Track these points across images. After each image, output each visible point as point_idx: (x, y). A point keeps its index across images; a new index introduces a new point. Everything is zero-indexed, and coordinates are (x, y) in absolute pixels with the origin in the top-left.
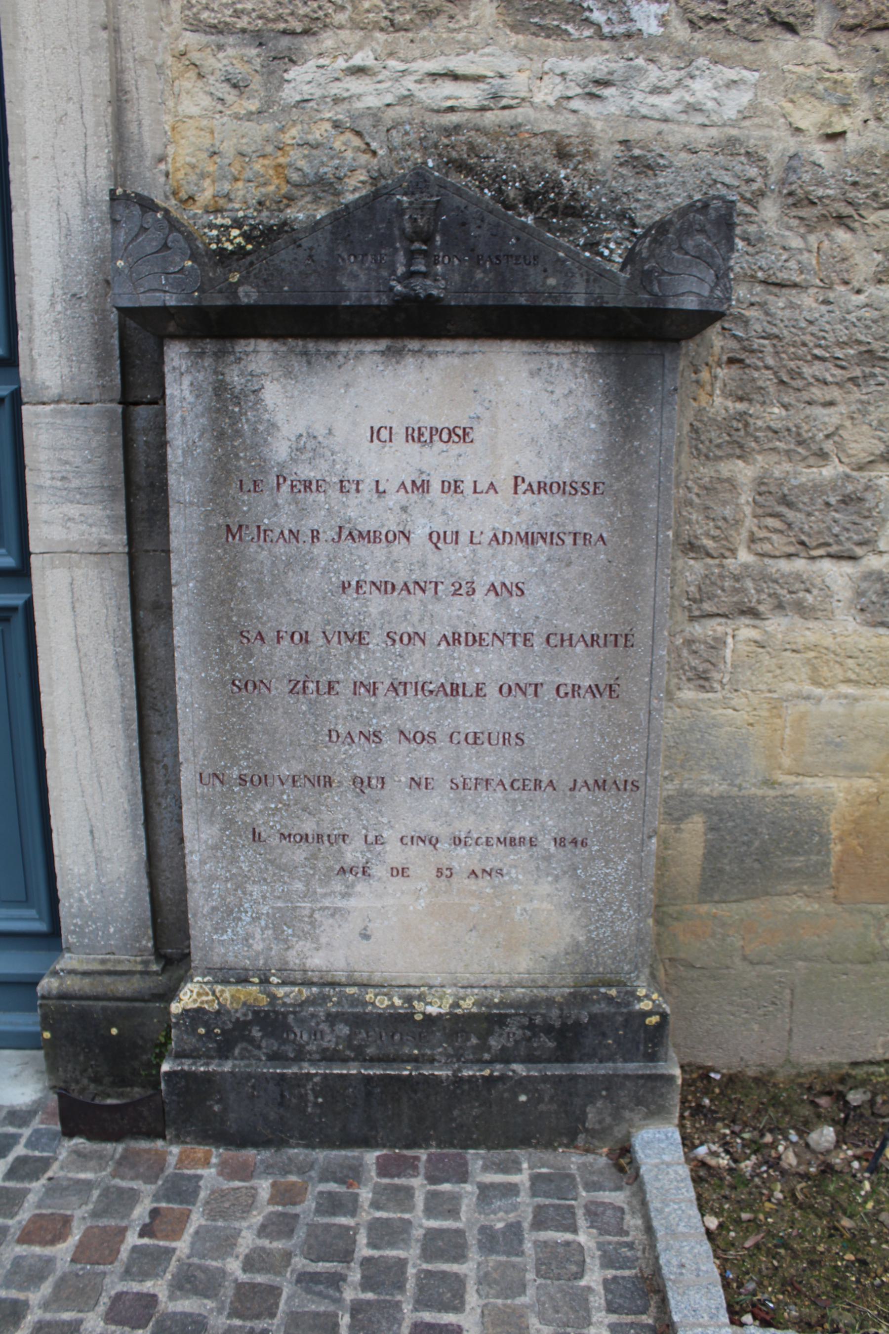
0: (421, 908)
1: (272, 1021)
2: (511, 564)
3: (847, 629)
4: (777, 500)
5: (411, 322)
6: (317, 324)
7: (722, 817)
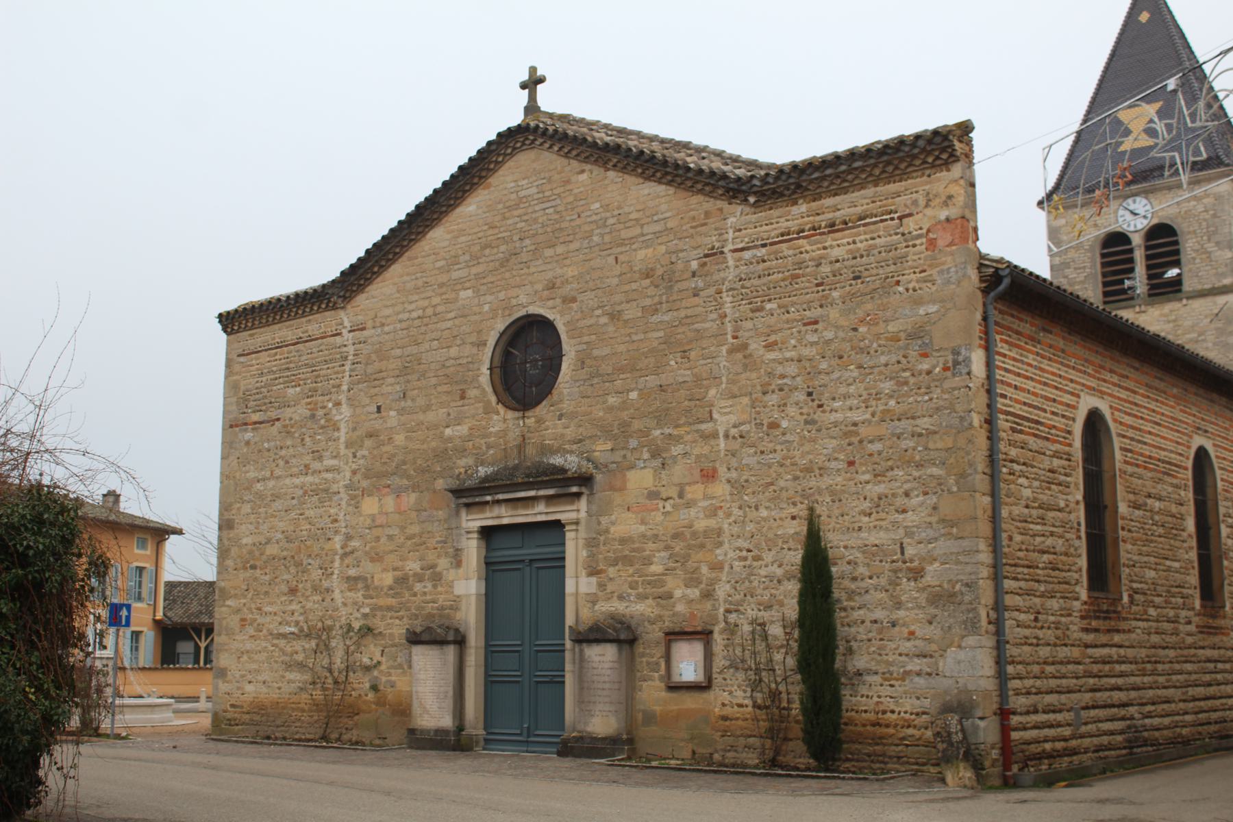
0: (602, 723)
1: (582, 738)
2: (609, 672)
3: (657, 683)
4: (648, 663)
5: (598, 641)
6: (590, 641)
7: (644, 712)
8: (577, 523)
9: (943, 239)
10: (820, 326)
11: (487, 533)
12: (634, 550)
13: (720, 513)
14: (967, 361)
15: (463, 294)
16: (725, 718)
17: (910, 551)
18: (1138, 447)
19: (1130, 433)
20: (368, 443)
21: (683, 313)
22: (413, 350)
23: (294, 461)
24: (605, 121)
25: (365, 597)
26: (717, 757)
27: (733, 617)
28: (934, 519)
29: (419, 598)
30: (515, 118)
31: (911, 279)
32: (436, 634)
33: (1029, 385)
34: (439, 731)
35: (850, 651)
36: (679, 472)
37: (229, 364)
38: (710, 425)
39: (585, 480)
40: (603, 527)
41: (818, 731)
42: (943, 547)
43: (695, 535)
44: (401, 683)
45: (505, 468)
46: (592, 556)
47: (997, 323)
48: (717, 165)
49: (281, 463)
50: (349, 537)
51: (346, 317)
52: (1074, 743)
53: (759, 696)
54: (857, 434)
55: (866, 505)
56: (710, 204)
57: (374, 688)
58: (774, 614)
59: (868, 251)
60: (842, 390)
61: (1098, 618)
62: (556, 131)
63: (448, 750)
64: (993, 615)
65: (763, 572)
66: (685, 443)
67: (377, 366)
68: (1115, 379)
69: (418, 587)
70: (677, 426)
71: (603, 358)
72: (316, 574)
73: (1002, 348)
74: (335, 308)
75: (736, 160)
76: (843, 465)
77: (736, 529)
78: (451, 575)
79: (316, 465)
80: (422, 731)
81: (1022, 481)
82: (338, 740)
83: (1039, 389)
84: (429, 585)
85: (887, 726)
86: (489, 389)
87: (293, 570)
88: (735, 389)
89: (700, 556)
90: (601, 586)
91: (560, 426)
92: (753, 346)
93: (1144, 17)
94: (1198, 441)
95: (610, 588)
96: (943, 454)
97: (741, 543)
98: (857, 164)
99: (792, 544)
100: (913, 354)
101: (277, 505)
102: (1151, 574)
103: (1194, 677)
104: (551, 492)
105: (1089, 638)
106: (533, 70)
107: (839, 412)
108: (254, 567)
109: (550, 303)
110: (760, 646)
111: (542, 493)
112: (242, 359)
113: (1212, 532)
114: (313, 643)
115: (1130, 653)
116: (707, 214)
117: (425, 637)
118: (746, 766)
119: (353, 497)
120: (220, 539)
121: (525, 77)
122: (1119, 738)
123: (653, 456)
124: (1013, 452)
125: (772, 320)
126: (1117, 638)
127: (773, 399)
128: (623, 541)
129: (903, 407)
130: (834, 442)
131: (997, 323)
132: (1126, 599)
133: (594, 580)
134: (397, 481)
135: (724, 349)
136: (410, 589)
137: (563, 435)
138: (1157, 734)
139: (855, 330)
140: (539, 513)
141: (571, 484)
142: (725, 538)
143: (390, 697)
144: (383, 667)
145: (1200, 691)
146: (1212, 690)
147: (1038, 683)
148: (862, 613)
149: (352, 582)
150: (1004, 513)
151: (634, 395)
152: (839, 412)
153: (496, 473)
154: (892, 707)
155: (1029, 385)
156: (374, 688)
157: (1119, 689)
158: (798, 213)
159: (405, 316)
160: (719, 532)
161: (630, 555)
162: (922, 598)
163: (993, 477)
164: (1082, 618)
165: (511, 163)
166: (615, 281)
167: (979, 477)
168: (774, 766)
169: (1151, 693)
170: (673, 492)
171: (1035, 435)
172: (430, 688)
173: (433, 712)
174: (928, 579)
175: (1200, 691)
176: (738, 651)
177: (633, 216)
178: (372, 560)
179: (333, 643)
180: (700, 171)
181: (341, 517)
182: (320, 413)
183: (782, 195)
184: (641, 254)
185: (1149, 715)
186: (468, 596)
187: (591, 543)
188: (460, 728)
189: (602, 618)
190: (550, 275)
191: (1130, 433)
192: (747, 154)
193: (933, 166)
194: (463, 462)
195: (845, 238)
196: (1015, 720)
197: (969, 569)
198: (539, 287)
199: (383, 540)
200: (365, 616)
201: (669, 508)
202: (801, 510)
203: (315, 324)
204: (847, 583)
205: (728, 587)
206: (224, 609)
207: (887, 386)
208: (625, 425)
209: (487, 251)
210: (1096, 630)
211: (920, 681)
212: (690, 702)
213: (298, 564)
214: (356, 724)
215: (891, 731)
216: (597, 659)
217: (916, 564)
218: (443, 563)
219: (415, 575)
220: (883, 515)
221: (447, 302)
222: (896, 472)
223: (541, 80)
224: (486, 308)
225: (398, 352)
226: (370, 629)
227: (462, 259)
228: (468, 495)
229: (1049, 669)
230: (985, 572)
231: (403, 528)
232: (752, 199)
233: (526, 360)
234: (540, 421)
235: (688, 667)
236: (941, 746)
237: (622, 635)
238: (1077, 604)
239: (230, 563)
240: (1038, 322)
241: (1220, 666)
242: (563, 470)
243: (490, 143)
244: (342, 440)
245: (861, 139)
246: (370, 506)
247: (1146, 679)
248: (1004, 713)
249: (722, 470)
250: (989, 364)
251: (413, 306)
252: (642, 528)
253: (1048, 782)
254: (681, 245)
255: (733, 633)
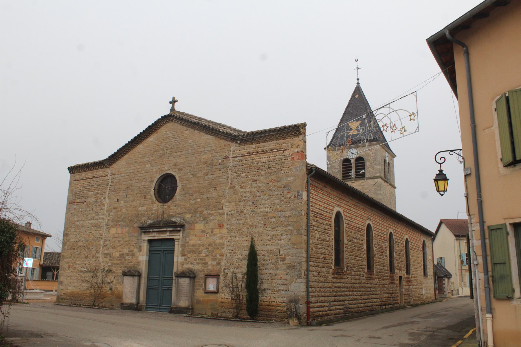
0: (183, 303)
3: (202, 291)
5: (183, 277)
6: (181, 277)
8: (179, 239)
9: (296, 158)
10: (257, 182)
11: (150, 241)
12: (196, 249)
13: (224, 238)
14: (302, 195)
15: (147, 166)
16: (222, 302)
17: (282, 252)
18: (351, 223)
19: (349, 219)
20: (114, 211)
21: (215, 176)
22: (130, 182)
23: (89, 215)
24: (195, 115)
26: (219, 315)
27: (226, 271)
28: (289, 243)
29: (127, 261)
30: (167, 112)
31: (286, 169)
32: (132, 273)
33: (320, 203)
34: (131, 304)
35: (262, 282)
36: (211, 225)
37: (70, 183)
38: (222, 210)
39: (182, 226)
40: (187, 241)
41: (251, 307)
42: (291, 251)
43: (215, 244)
44: (120, 289)
45: (157, 221)
46: (183, 250)
47: (311, 184)
48: (229, 131)
49: (85, 216)
50: (106, 241)
51: (109, 171)
52: (328, 312)
53: (233, 296)
54: (267, 215)
55: (269, 238)
56: (226, 143)
57: (111, 289)
58: (239, 270)
59: (273, 160)
60: (263, 202)
61: (337, 274)
62: (180, 117)
63: (133, 310)
64: (306, 273)
65: (236, 257)
66: (214, 216)
67: (118, 186)
68: (345, 202)
69: (127, 258)
70: (212, 211)
71: (190, 188)
72: (94, 252)
73: (312, 191)
74: (106, 168)
75: (234, 130)
76: (262, 225)
77: (228, 243)
78: (138, 254)
79: (96, 217)
80: (126, 304)
81: (316, 232)
82: (98, 306)
83: (322, 204)
84: (131, 257)
85: (272, 306)
86: (153, 196)
87: (87, 250)
88: (231, 200)
89: (217, 251)
90: (186, 260)
91: (174, 209)
92: (237, 187)
93: (357, 96)
94: (368, 222)
95: (188, 260)
96: (293, 223)
97: (230, 248)
98: (271, 134)
99: (245, 249)
100: (285, 192)
101: (83, 229)
102: (353, 261)
103: (364, 292)
104: (171, 229)
105: (334, 280)
106: (174, 98)
107: (262, 209)
108: (74, 249)
109: (174, 170)
110: (234, 280)
111: (168, 229)
112: (75, 182)
113: (371, 249)
114: (92, 274)
115: (346, 285)
116: (225, 146)
117: (128, 274)
118: (228, 318)
119: (108, 228)
120: (63, 239)
121: (171, 100)
122: (342, 311)
123: (204, 220)
124: (314, 223)
125: (243, 179)
126: (342, 280)
127: (242, 204)
128: (193, 246)
129: (280, 209)
130: (260, 218)
131: (311, 184)
132: (345, 269)
133: (183, 257)
134: (122, 223)
135: (228, 188)
136: (124, 258)
137: (176, 212)
138: (353, 310)
139: (268, 184)
140: (167, 236)
141: (177, 227)
142: (225, 246)
143: (116, 292)
144: (114, 283)
145: (366, 297)
146: (369, 297)
147: (319, 294)
148: (267, 271)
149: (106, 255)
150: (311, 242)
151: (199, 200)
152: (262, 209)
153: (154, 222)
154: (274, 300)
155: (320, 203)
156: (111, 289)
157: (342, 296)
158: (252, 147)
159: (128, 171)
160: (223, 244)
161: (195, 250)
162: (285, 267)
163: (308, 230)
164: (332, 274)
165: (165, 126)
166: (195, 164)
167: (304, 230)
168: (237, 318)
169: (352, 297)
170: (210, 231)
171: (321, 218)
172: (128, 290)
173: (130, 298)
174: (287, 261)
175: (366, 297)
176: (227, 282)
177: (202, 145)
178: (113, 248)
179: (98, 274)
180: (223, 132)
181: (103, 234)
182: (99, 200)
183: (248, 141)
184: (204, 157)
185: (351, 304)
186: (143, 261)
187: (183, 246)
188: (138, 303)
189: (185, 270)
190: (175, 161)
191: (349, 219)
192: (238, 128)
193: (294, 135)
194: (144, 218)
195: (266, 155)
196: (311, 305)
197: (299, 258)
198: (171, 165)
199: (117, 242)
200: (109, 266)
201: (208, 236)
202: (249, 238)
203: (99, 172)
204: (262, 261)
205: (225, 261)
207: (277, 201)
208: (195, 209)
209: (156, 153)
210: (336, 278)
211: (283, 292)
212: (212, 297)
213: (88, 249)
214: (104, 301)
215: (274, 308)
216: (183, 283)
217: (283, 256)
218: (135, 250)
219: (126, 254)
220: (274, 241)
221: (142, 168)
222: (278, 228)
223: (176, 101)
224: (154, 170)
225: (125, 183)
226: (110, 270)
227: (148, 155)
228: (145, 229)
229: (322, 289)
230: (304, 259)
231: (123, 239)
232: (239, 142)
233: (166, 187)
234: (169, 207)
235: (211, 286)
236: (288, 313)
237: (191, 275)
238: (331, 270)
239: (66, 247)
240: (323, 184)
241: (372, 289)
242: (175, 223)
243: (159, 119)
244: (106, 209)
245: (273, 126)
246: (113, 231)
247: (350, 293)
248: (308, 303)
249: (225, 225)
250: (308, 196)
251: (131, 169)
252: (199, 242)
253: (320, 324)
254: (216, 155)
255: (226, 276)
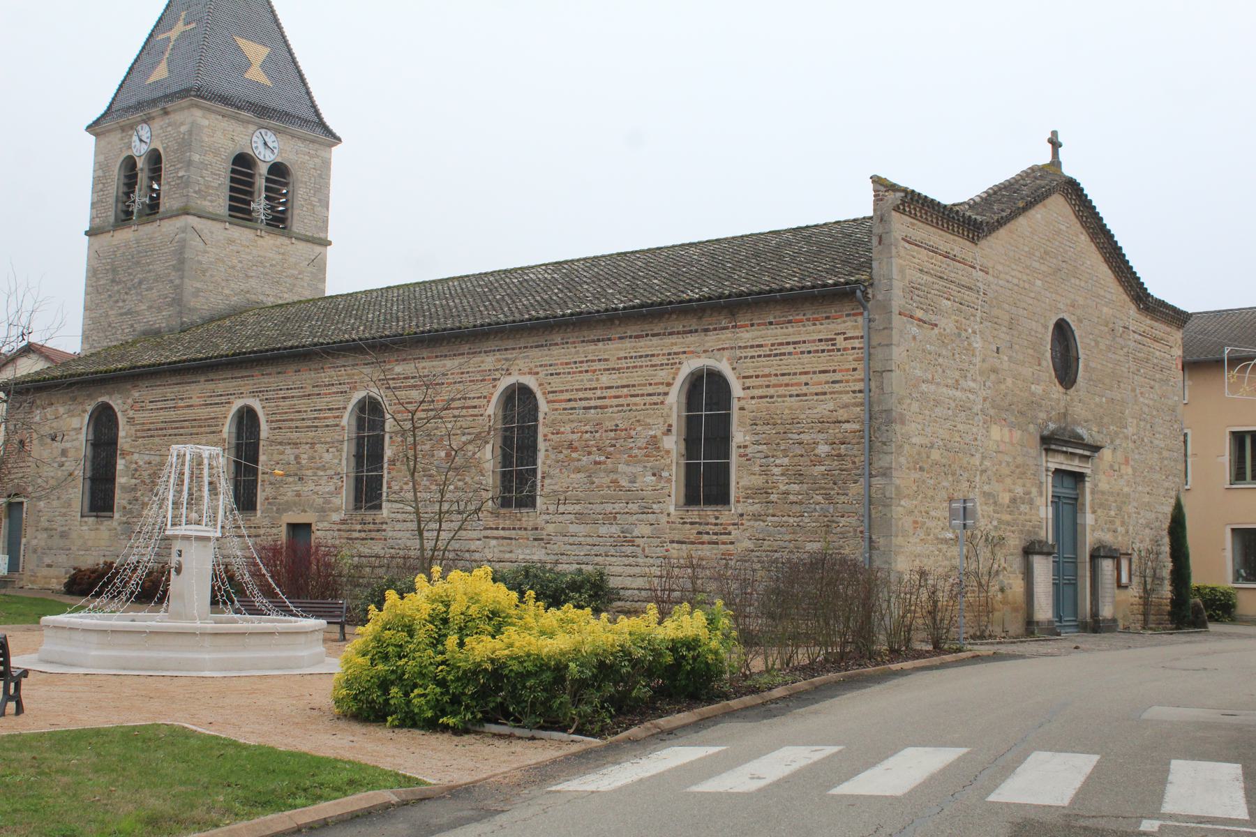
20: (993, 377)
25: (995, 512)
50: (984, 458)
57: (1002, 590)
82: (980, 637)
108: (921, 469)
199: (1004, 464)
202: (1173, 494)
206: (900, 509)
